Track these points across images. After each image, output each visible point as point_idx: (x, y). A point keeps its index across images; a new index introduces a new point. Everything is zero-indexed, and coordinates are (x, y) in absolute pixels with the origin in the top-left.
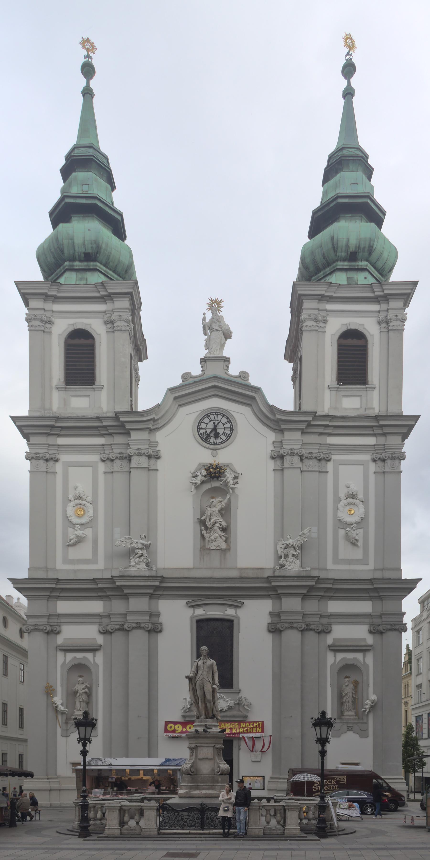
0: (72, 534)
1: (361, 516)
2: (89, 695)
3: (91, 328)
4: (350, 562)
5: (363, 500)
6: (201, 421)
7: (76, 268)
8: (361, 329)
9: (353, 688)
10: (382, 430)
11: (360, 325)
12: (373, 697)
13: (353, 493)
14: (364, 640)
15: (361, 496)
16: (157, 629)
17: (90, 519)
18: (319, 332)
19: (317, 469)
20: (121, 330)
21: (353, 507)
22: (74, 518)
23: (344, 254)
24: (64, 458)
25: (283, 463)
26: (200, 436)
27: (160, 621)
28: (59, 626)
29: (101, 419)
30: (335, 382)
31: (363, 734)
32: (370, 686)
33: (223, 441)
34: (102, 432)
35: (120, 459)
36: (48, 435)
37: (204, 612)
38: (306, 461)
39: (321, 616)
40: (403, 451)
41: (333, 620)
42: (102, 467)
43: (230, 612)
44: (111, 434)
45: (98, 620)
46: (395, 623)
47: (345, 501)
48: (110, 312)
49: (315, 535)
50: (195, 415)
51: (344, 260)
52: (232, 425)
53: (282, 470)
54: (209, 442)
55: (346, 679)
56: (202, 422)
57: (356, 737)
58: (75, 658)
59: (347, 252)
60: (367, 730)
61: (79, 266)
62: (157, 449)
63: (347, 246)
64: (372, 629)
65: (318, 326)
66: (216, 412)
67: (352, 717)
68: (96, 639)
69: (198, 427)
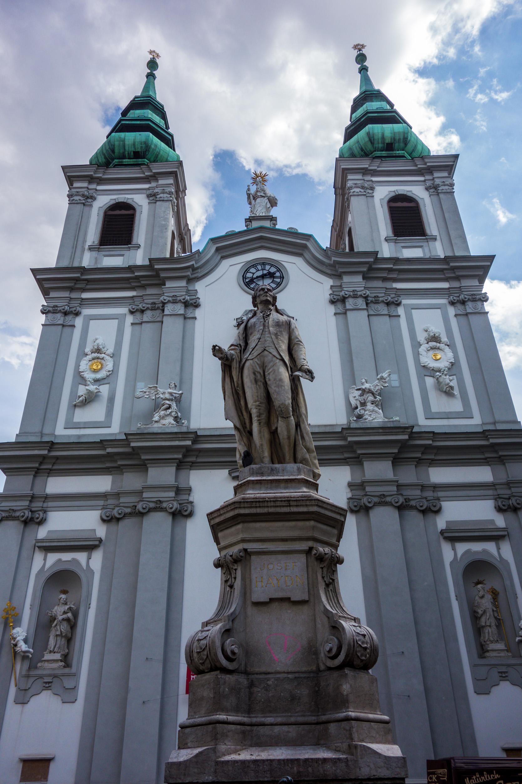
0: (82, 390)
1: (450, 361)
2: (72, 624)
4: (448, 416)
5: (448, 343)
6: (247, 271)
7: (125, 163)
8: (409, 194)
9: (492, 601)
10: (455, 273)
11: (407, 191)
13: (435, 335)
14: (492, 522)
15: (444, 339)
16: (186, 511)
17: (108, 374)
18: (367, 197)
19: (387, 313)
20: (163, 200)
21: (437, 352)
22: (88, 374)
23: (380, 145)
24: (87, 312)
25: (345, 307)
27: (191, 499)
28: (45, 512)
29: (133, 269)
30: (390, 234)
32: (518, 595)
35: (152, 310)
36: (71, 289)
38: (372, 305)
39: (423, 487)
40: (483, 292)
41: (440, 494)
42: (130, 319)
44: (143, 287)
45: (101, 503)
47: (427, 345)
49: (396, 384)
51: (382, 151)
52: (282, 274)
53: (345, 313)
55: (479, 586)
56: (248, 272)
58: (60, 560)
59: (384, 143)
61: (128, 162)
63: (383, 137)
64: (500, 504)
65: (365, 192)
66: (263, 263)
68: (95, 530)
69: (243, 276)
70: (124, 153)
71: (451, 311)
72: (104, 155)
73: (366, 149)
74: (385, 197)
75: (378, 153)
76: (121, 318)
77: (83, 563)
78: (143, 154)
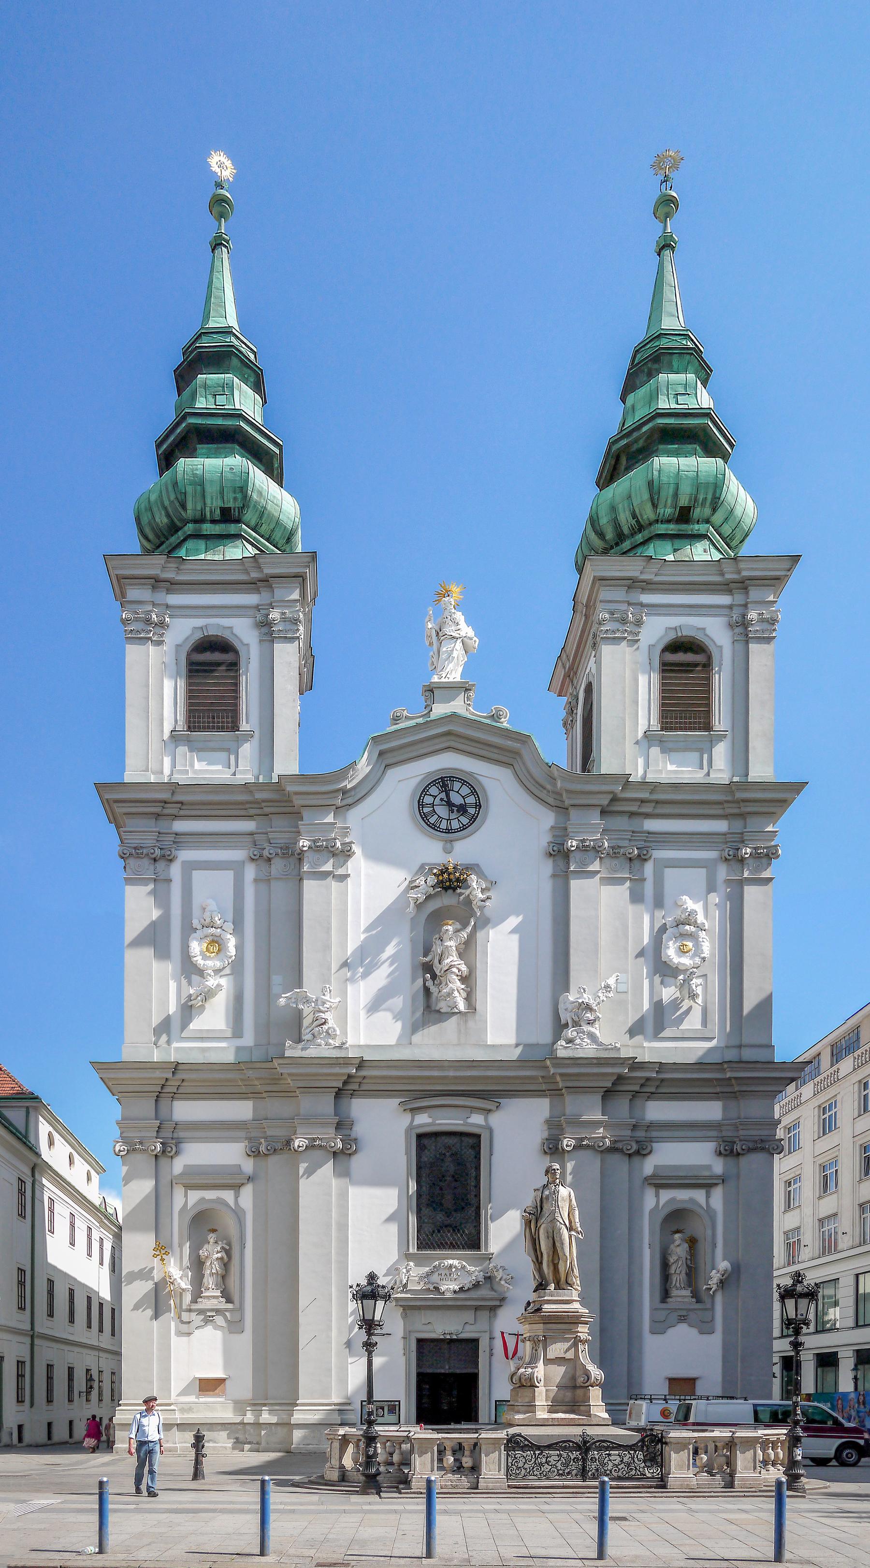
3: (232, 633)
6: (425, 792)
11: (698, 629)
12: (724, 1265)
14: (709, 1167)
23: (669, 511)
24: (185, 855)
26: (423, 818)
31: (706, 1328)
33: (464, 825)
34: (252, 812)
36: (157, 816)
37: (430, 1120)
41: (654, 1134)
43: (477, 1119)
46: (763, 1138)
47: (675, 930)
48: (267, 607)
50: (414, 782)
51: (668, 521)
54: (439, 827)
55: (677, 1236)
56: (426, 794)
57: (694, 1332)
60: (713, 1320)
62: (347, 840)
67: (686, 1300)
69: (419, 802)
70: (203, 511)
71: (722, 872)
72: (165, 508)
73: (641, 515)
74: (658, 641)
75: (662, 528)
76: (237, 868)
77: (231, 1202)
78: (237, 514)
